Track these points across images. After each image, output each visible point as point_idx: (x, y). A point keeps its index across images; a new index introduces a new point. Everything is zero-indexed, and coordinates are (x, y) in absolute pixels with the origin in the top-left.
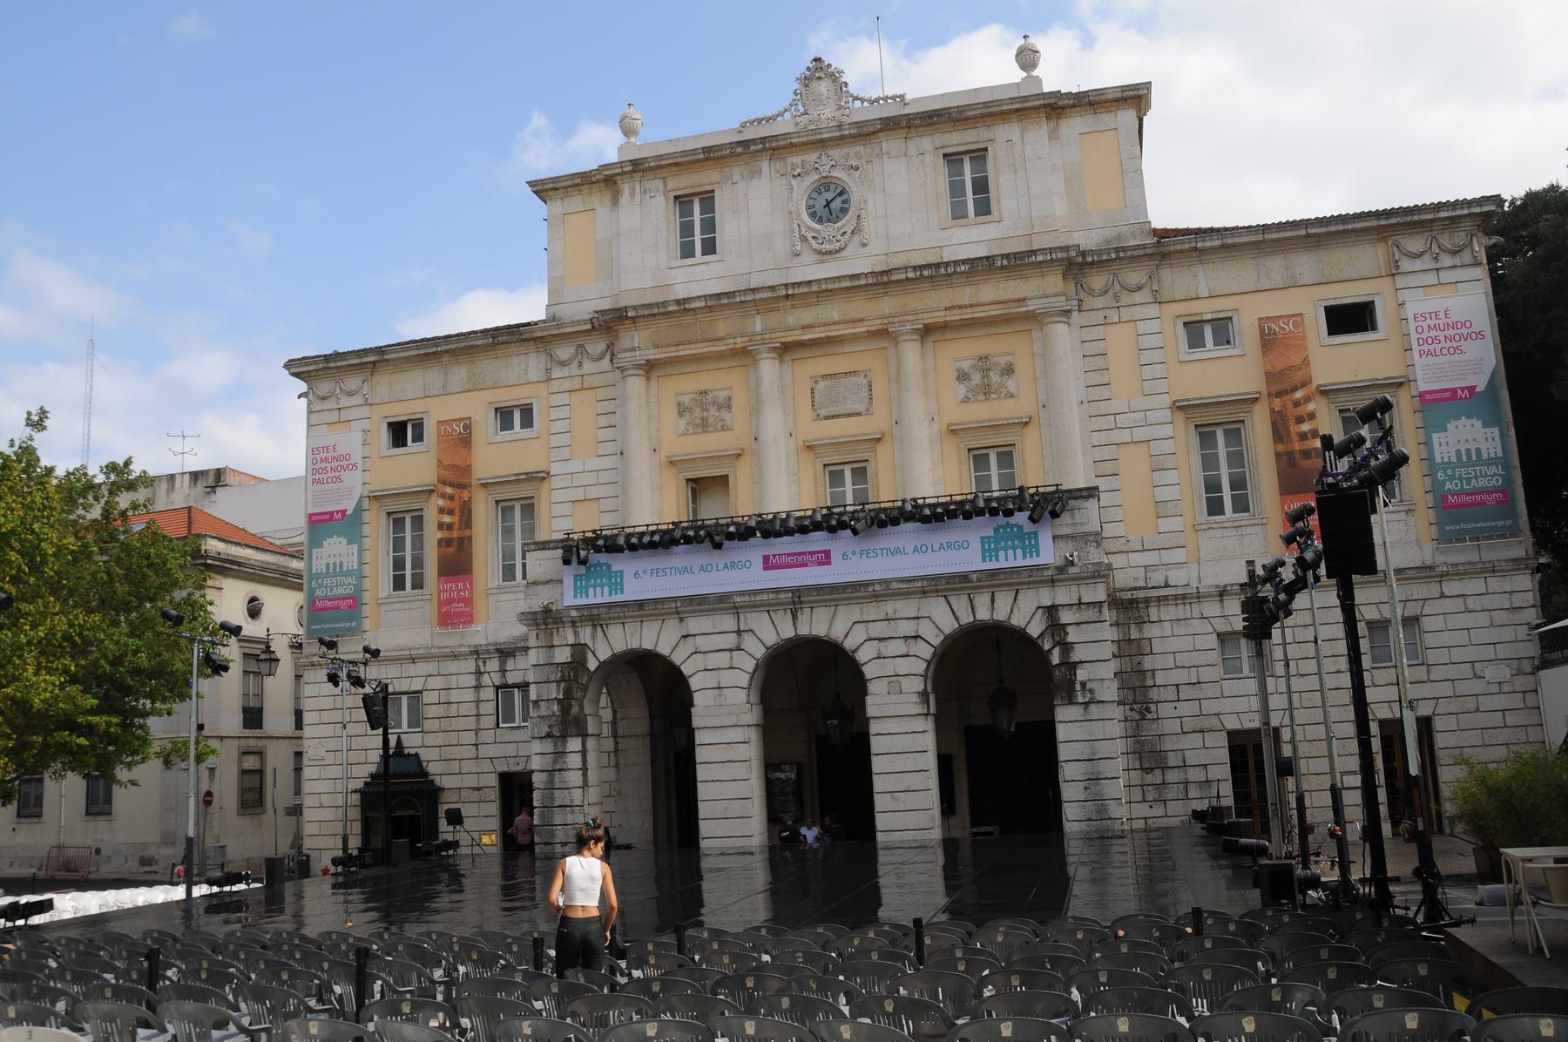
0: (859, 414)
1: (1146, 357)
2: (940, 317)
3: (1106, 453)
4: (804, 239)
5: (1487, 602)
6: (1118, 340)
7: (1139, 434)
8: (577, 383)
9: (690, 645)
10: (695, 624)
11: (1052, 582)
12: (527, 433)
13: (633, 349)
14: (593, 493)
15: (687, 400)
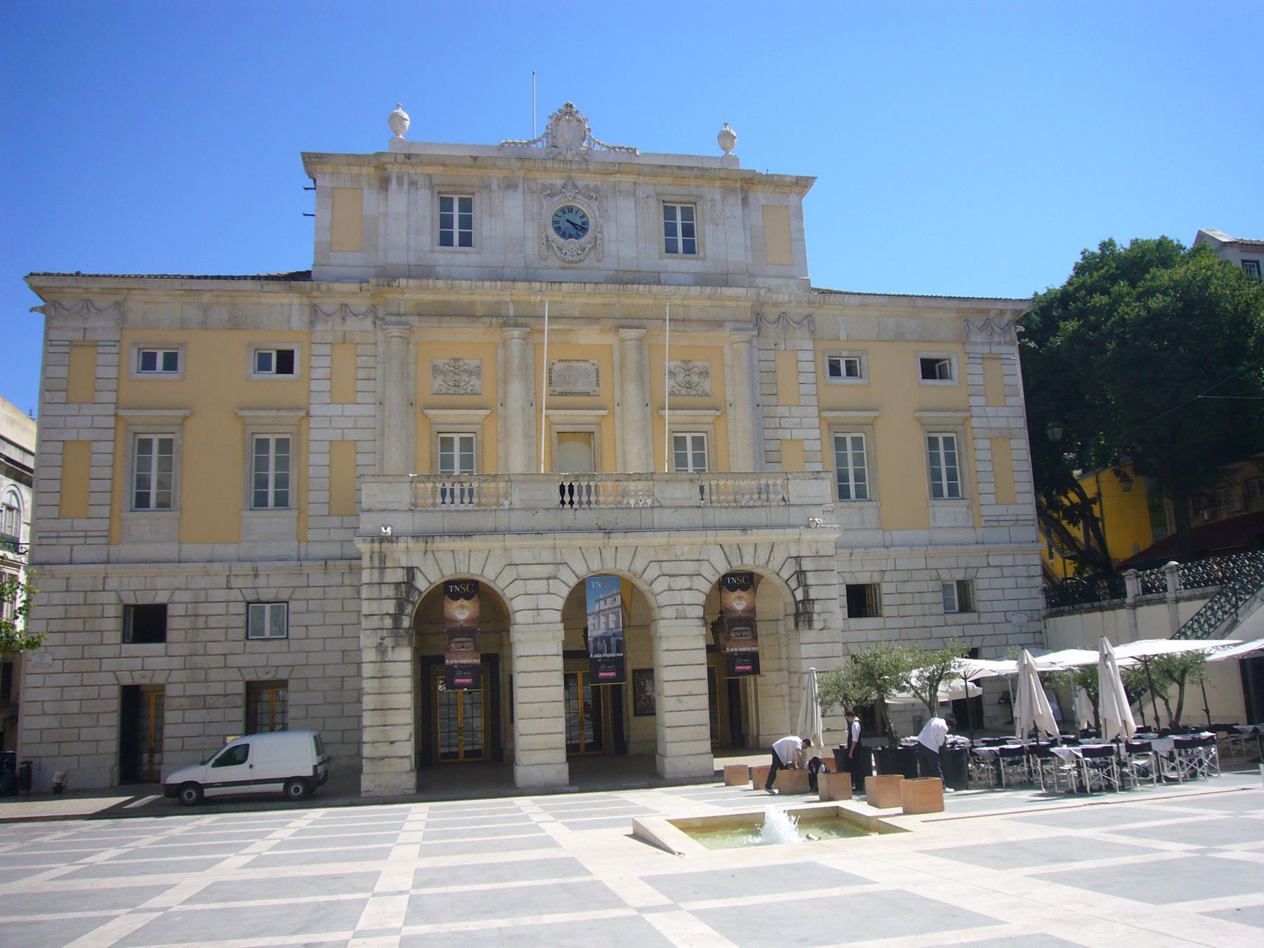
0: (588, 394)
1: (802, 378)
3: (773, 445)
4: (549, 247)
7: (797, 434)
9: (510, 574)
13: (399, 315)
14: (351, 435)
15: (440, 363)
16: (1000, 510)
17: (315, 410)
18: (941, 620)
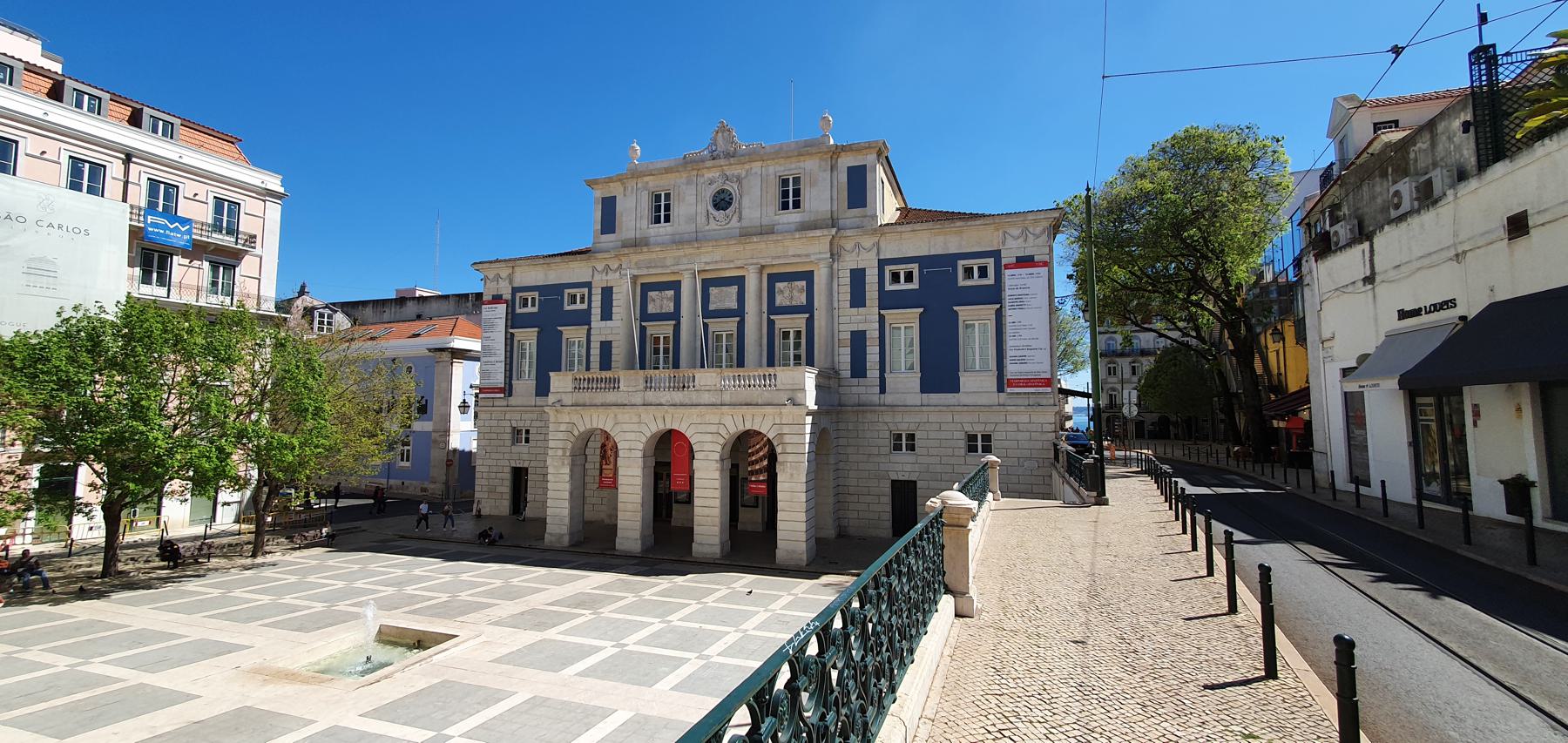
5: (1029, 427)
9: (618, 429)
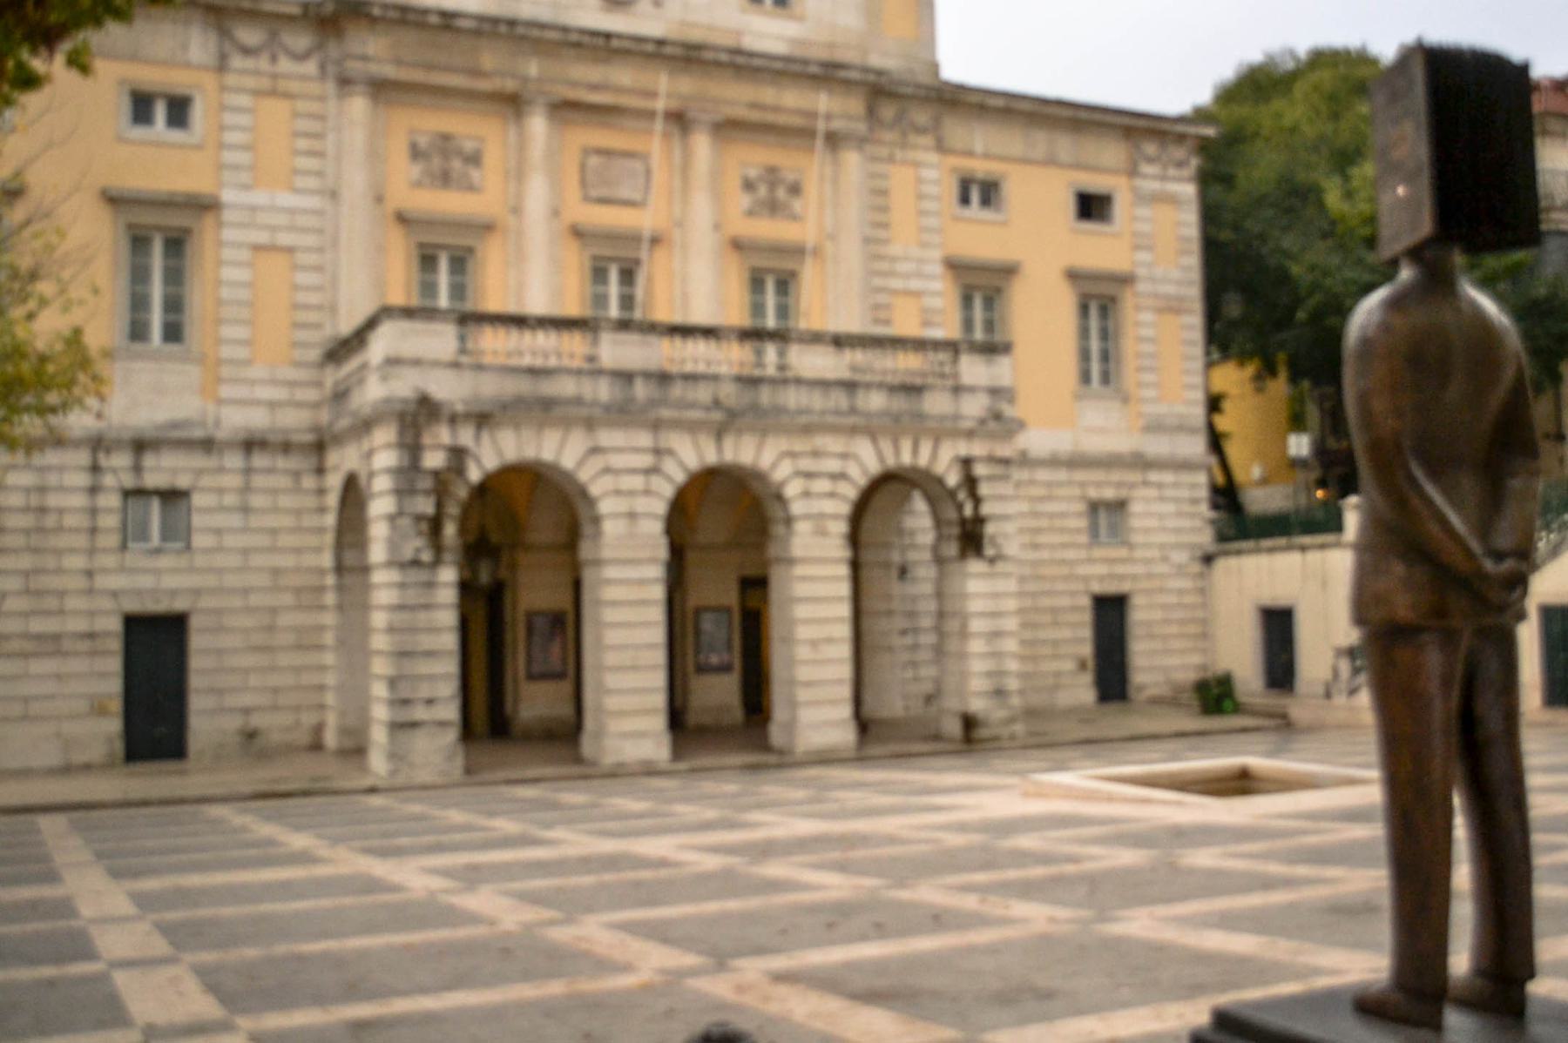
2: (741, 113)
3: (882, 298)
6: (900, 179)
7: (915, 284)
8: (265, 83)
9: (597, 463)
10: (607, 437)
11: (970, 434)
12: (176, 135)
14: (285, 239)
15: (423, 141)
16: (1160, 409)
17: (227, 196)
18: (1083, 554)
